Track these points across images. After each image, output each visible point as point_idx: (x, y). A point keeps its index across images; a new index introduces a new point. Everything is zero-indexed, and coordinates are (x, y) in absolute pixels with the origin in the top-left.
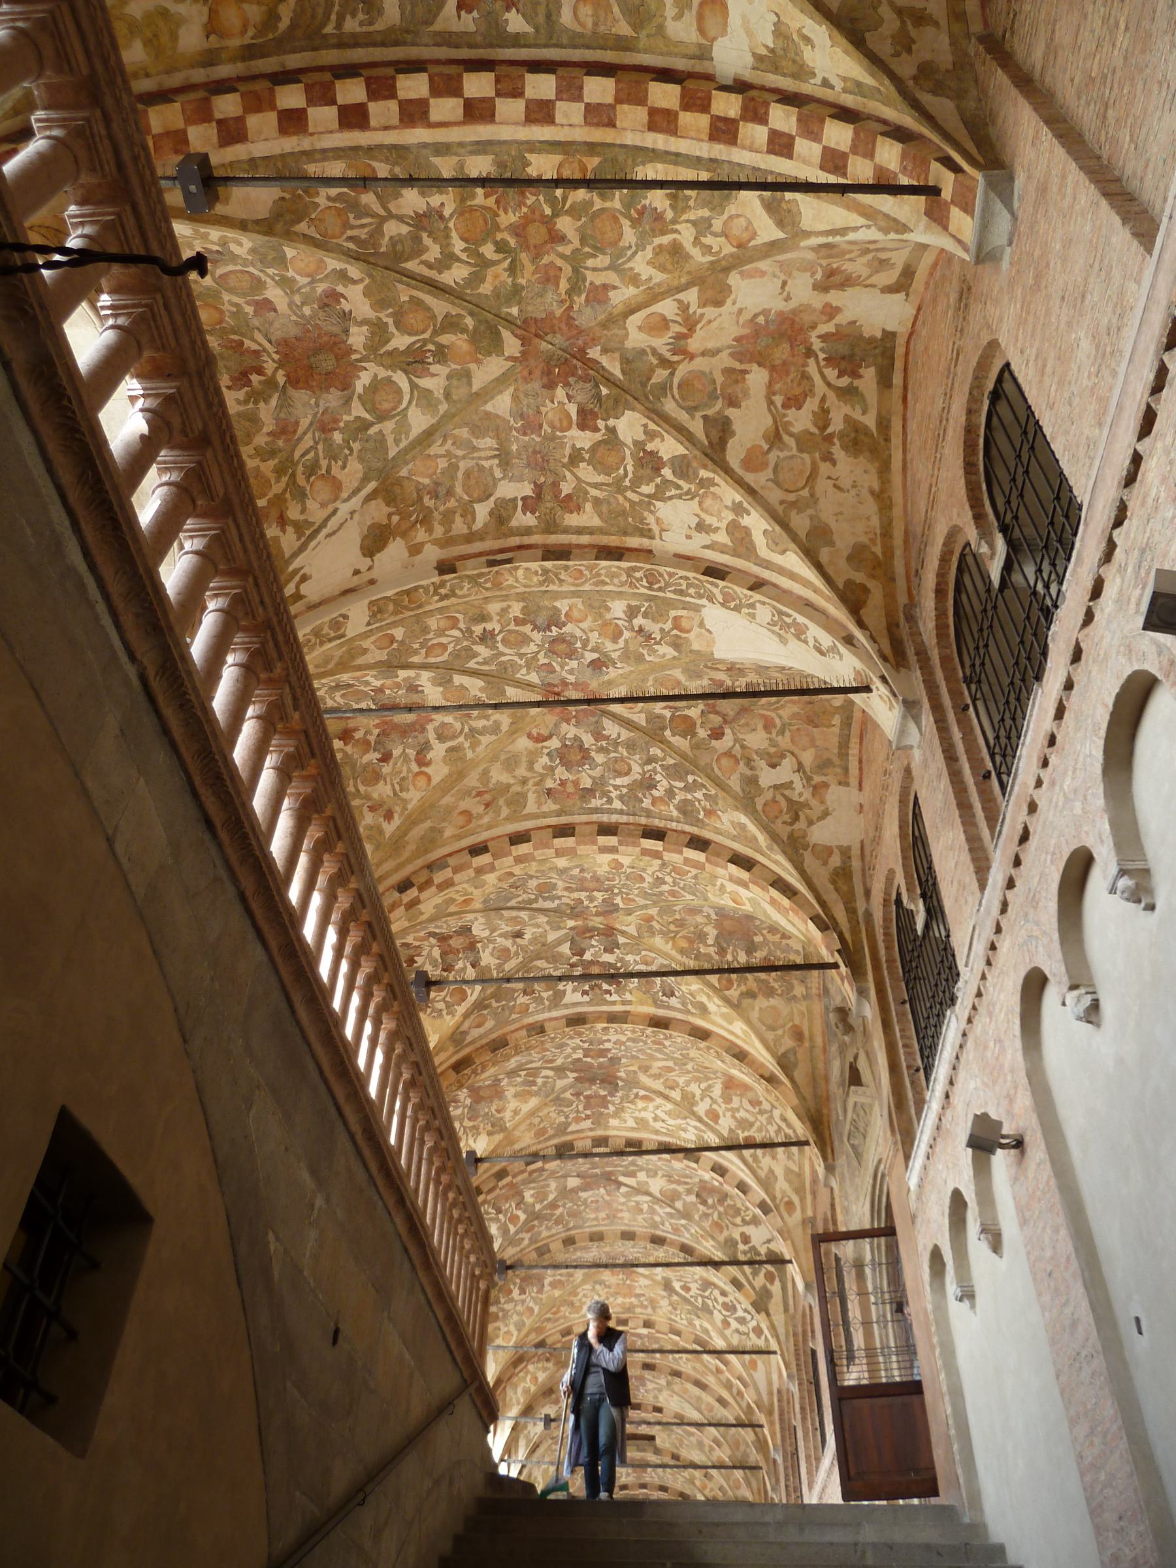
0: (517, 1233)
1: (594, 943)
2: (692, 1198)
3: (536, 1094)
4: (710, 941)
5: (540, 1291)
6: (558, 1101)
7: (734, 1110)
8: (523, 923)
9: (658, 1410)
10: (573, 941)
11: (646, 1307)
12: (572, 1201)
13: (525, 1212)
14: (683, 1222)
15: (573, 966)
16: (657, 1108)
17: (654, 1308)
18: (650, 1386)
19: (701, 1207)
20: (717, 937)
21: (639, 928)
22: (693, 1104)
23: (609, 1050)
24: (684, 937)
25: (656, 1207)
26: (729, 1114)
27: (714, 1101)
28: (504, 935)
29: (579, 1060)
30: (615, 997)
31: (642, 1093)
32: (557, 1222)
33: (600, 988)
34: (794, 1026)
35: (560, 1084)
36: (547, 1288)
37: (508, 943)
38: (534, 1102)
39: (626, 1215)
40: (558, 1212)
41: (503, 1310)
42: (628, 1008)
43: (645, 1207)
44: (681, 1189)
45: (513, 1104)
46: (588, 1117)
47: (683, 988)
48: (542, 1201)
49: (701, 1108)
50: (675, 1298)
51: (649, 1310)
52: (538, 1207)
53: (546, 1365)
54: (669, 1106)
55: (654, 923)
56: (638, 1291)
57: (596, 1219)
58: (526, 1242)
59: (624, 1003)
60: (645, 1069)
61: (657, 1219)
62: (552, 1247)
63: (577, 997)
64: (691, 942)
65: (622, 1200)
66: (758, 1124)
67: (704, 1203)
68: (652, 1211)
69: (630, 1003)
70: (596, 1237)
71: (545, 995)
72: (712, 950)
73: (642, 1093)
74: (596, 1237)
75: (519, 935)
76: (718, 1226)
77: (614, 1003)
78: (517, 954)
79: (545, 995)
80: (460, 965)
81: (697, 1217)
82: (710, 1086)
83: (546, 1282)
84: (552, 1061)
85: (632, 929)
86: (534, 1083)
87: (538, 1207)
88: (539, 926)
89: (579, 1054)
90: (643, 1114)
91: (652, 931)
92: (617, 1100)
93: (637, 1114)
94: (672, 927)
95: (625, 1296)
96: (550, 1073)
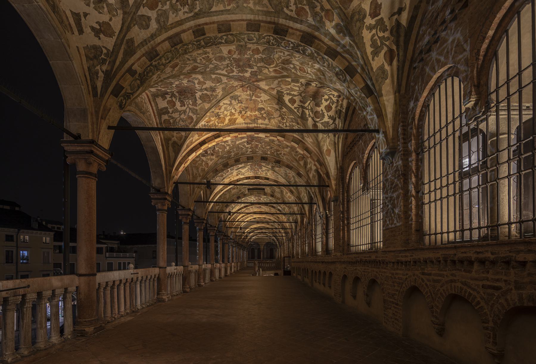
9: (268, 179)
11: (264, 119)
17: (269, 119)
18: (264, 169)
36: (199, 101)
41: (173, 118)
50: (284, 110)
51: (267, 121)
53: (212, 157)
56: (260, 106)
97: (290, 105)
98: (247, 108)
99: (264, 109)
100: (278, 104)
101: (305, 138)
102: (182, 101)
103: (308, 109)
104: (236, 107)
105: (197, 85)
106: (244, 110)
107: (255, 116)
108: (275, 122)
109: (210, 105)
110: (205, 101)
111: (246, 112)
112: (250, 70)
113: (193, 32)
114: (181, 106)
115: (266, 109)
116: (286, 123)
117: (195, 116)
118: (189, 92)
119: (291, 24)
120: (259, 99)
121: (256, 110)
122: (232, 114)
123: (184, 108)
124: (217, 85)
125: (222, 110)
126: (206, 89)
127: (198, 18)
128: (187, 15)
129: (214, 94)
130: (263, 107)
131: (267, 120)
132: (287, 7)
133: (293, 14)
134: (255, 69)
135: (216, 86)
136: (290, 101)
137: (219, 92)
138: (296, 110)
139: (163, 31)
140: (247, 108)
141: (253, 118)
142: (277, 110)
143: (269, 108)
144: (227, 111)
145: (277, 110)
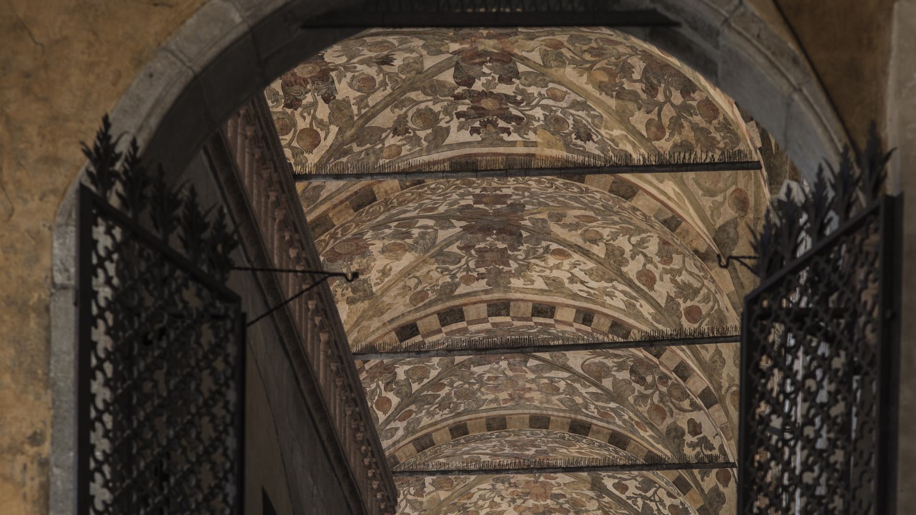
0: (388, 421)
1: (485, 70)
2: (625, 375)
3: (411, 248)
4: (636, 76)
6: (442, 256)
7: (674, 273)
8: (391, 46)
10: (457, 67)
12: (462, 378)
13: (397, 394)
14: (613, 405)
15: (458, 98)
16: (575, 265)
19: (637, 387)
20: (645, 71)
21: (544, 56)
22: (623, 262)
23: (508, 196)
24: (603, 69)
25: (577, 385)
26: (667, 277)
27: (649, 260)
28: (368, 62)
29: (468, 207)
30: (515, 137)
31: (554, 246)
32: (441, 407)
33: (495, 125)
34: (737, 190)
35: (443, 235)
37: (372, 71)
38: (408, 259)
39: (536, 395)
40: (443, 393)
42: (532, 150)
43: (562, 385)
44: (609, 362)
45: (380, 262)
46: (481, 276)
47: (603, 131)
48: (420, 380)
49: (632, 269)
50: (607, 499)
52: (415, 387)
54: (590, 265)
55: (564, 51)
56: (556, 491)
57: (496, 400)
58: (400, 433)
59: (527, 144)
60: (558, 218)
61: (579, 400)
62: (436, 437)
63: (465, 136)
64: (612, 75)
65: (531, 376)
66: (704, 291)
67: (641, 381)
68: (572, 391)
69: (534, 144)
70: (497, 424)
71: (422, 134)
72: (638, 87)
73: (554, 246)
74: (497, 424)
75: (387, 61)
76: (659, 411)
77: (513, 144)
78: (384, 84)
79: (422, 134)
80: (309, 98)
81: (631, 399)
82: (643, 241)
84: (432, 209)
85: (536, 57)
86: (408, 235)
87: (415, 387)
88: (411, 50)
89: (469, 200)
90: (555, 273)
91: (562, 61)
92: (521, 255)
93: (547, 273)
94: (587, 57)
95: (537, 497)
96: (431, 223)
97: (617, 493)
99: (563, 496)
100: (592, 489)
103: (654, 501)
104: (504, 493)
106: (520, 498)
107: (546, 506)
109: (450, 493)
110: (442, 487)
113: (451, 430)
115: (567, 496)
119: (594, 421)
120: (553, 482)
121: (547, 498)
122: (493, 504)
125: (474, 499)
128: (444, 417)
132: (586, 409)
133: (596, 415)
136: (615, 486)
138: (630, 502)
140: (527, 494)
141: (541, 510)
142: (593, 498)
143: (574, 495)
144: (484, 500)
145: (593, 498)
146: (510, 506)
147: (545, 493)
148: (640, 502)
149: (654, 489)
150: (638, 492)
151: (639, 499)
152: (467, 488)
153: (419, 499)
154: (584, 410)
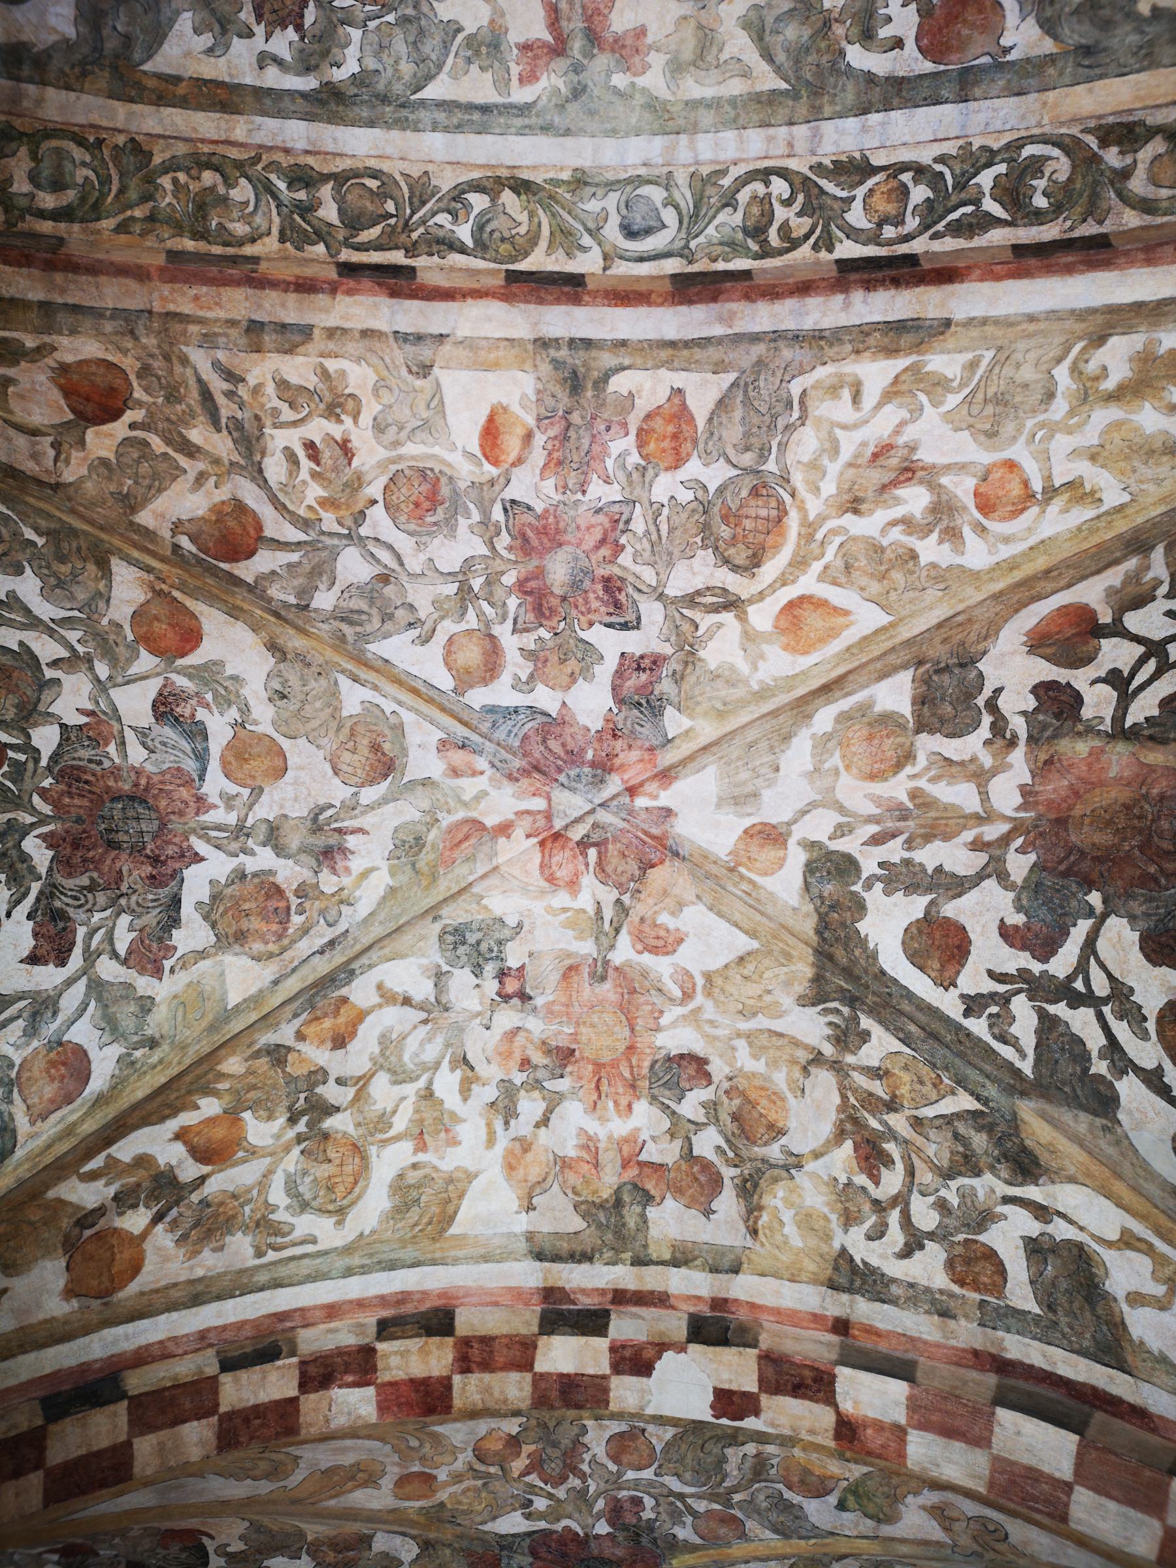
5: (150, 954)
36: (193, 933)
50: (881, 1044)
56: (676, 1038)
83: (196, 885)
98: (564, 1056)
100: (817, 995)
101: (1142, 1324)
102: (58, 916)
103: (1087, 999)
105: (215, 783)
107: (629, 1152)
108: (806, 1221)
109: (267, 972)
110: (241, 937)
111: (554, 1101)
112: (610, 644)
114: (33, 959)
115: (718, 1068)
116: (901, 1200)
117: (116, 1050)
118: (137, 850)
123: (48, 977)
124: (369, 794)
126: (273, 835)
127: (335, 119)
129: (328, 882)
130: (699, 1047)
131: (727, 1203)
132: (867, 37)
134: (649, 638)
135: (351, 807)
137: (369, 874)
138: (978, 1027)
139: (103, 79)
141: (609, 1180)
144: (400, 1077)
145: (818, 1059)
146: (491, 1141)
147: (631, 1048)
148: (1024, 1017)
149: (1082, 928)
150: (1016, 960)
151: (1023, 1009)
152: (338, 958)
153: (144, 984)
154: (858, 57)
